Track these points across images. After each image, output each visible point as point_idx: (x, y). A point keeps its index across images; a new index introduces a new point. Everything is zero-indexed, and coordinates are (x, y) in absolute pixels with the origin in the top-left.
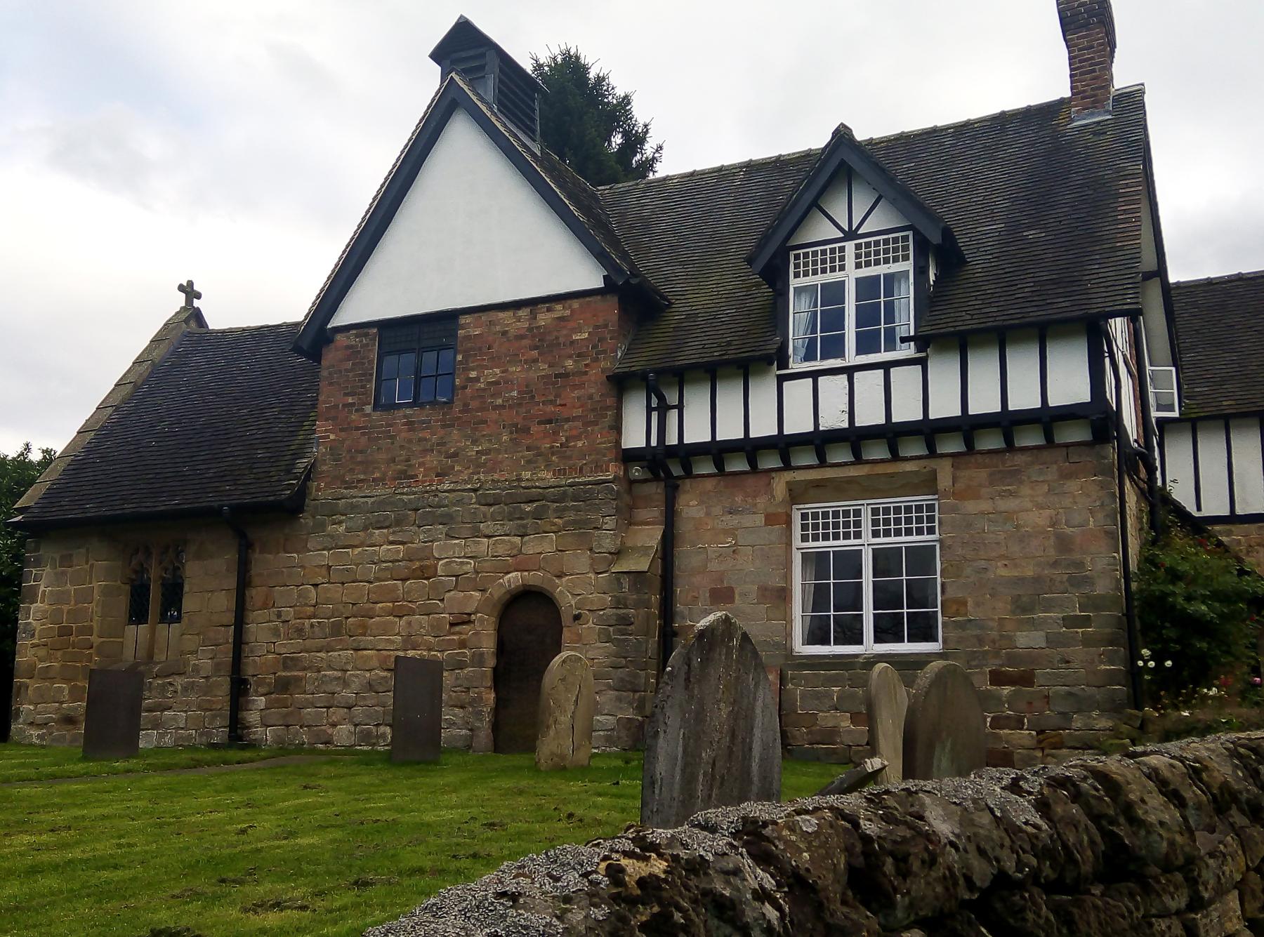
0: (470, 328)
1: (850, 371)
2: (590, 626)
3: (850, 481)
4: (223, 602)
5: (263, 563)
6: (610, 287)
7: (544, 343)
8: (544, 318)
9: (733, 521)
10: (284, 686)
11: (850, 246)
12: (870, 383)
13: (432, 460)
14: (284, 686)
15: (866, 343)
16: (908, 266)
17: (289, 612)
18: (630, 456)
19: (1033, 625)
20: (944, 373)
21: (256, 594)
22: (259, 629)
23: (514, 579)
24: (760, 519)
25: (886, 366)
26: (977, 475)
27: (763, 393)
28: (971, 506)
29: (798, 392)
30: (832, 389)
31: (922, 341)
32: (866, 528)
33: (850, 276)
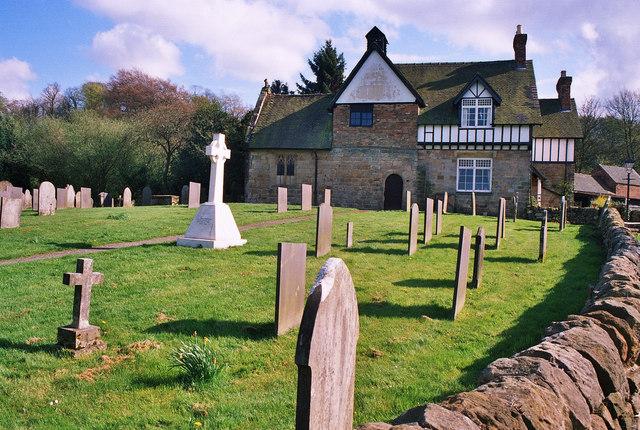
1: (476, 129)
5: (321, 162)
13: (367, 140)
15: (480, 123)
18: (420, 144)
23: (391, 171)
25: (485, 129)
27: (455, 129)
28: (501, 162)
29: (463, 133)
31: (493, 125)
33: (477, 107)
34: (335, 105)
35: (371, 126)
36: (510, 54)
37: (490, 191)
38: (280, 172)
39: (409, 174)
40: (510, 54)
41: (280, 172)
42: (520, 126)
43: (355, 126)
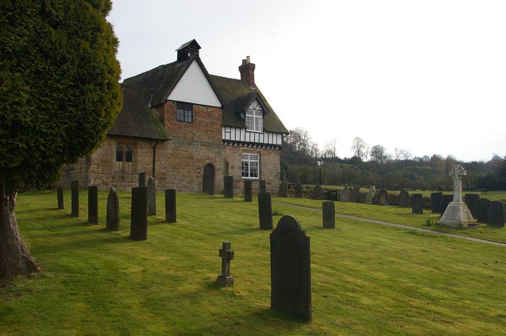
1: (255, 133)
2: (220, 172)
3: (250, 150)
4: (148, 159)
5: (158, 151)
6: (222, 107)
7: (209, 115)
8: (209, 110)
10: (162, 179)
11: (254, 111)
13: (190, 135)
14: (162, 179)
16: (262, 117)
20: (266, 135)
21: (156, 158)
23: (207, 161)
26: (266, 152)
28: (265, 157)
32: (249, 158)
36: (237, 76)
39: (219, 165)
40: (237, 76)
41: (119, 159)
43: (180, 121)
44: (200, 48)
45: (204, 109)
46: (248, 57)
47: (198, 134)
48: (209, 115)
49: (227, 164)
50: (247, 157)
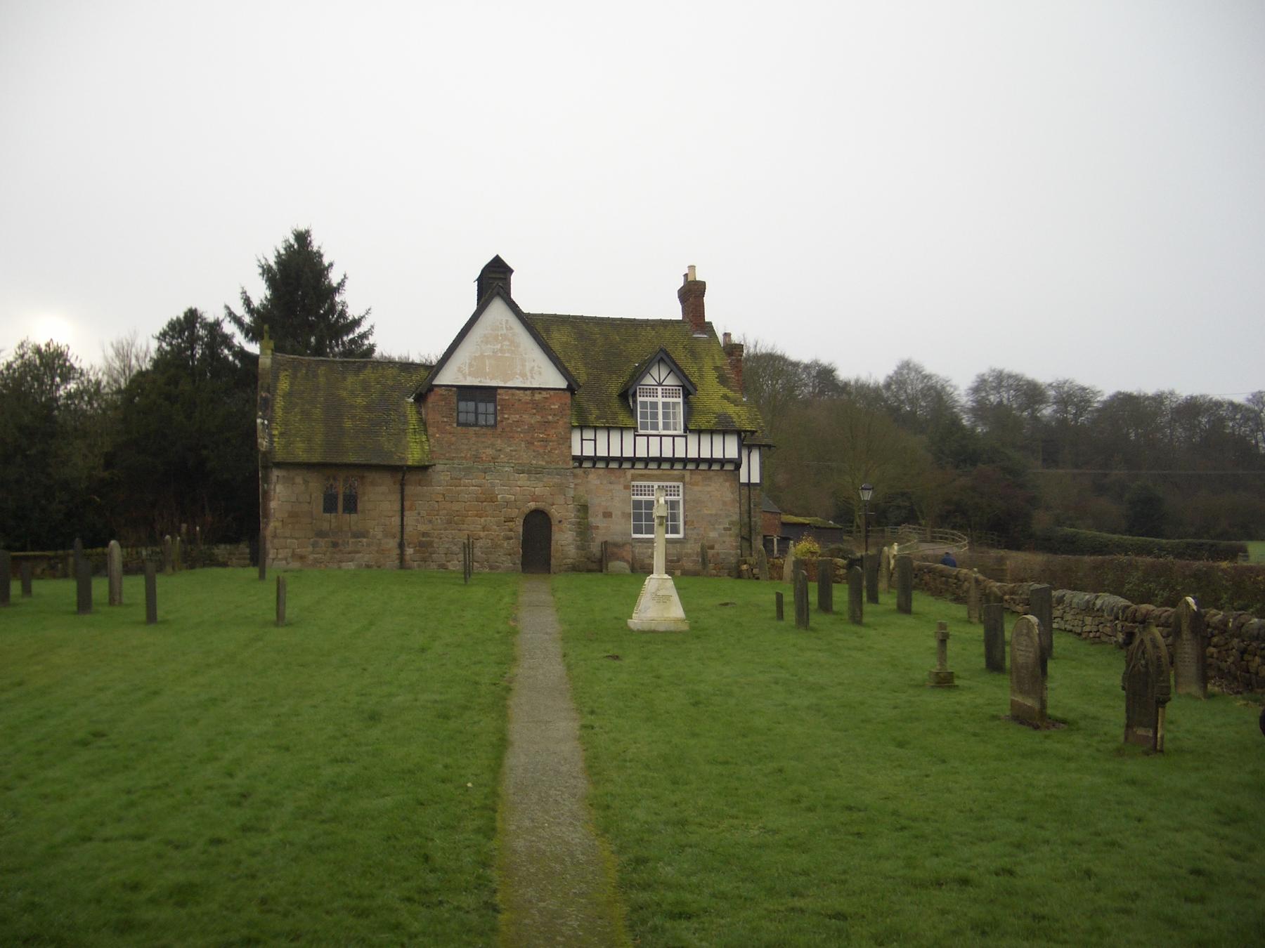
0: (501, 396)
1: (661, 436)
5: (409, 490)
6: (571, 389)
8: (537, 397)
9: (612, 487)
12: (667, 442)
13: (490, 451)
14: (422, 545)
15: (666, 427)
16: (680, 400)
17: (423, 513)
18: (575, 458)
19: (715, 529)
20: (693, 440)
21: (407, 504)
22: (410, 518)
23: (532, 505)
24: (621, 487)
25: (674, 436)
26: (697, 478)
27: (628, 437)
28: (696, 488)
29: (641, 441)
30: (654, 442)
33: (660, 400)
34: (432, 388)
35: (495, 426)
36: (674, 311)
37: (680, 536)
38: (330, 506)
40: (674, 311)
42: (724, 433)
43: (466, 425)
44: (511, 271)
45: (527, 397)
46: (692, 268)
47: (508, 449)
48: (538, 407)
49: (584, 509)
50: (650, 491)
